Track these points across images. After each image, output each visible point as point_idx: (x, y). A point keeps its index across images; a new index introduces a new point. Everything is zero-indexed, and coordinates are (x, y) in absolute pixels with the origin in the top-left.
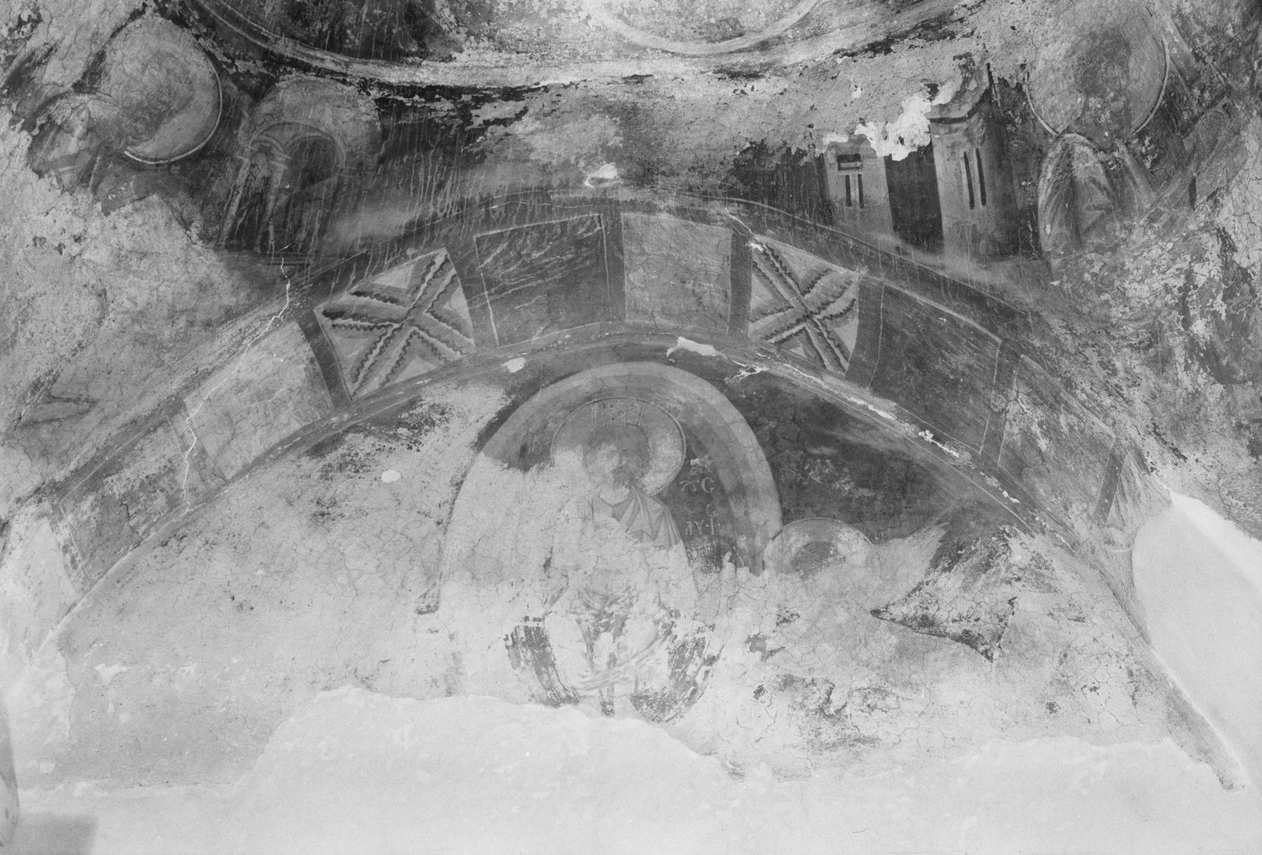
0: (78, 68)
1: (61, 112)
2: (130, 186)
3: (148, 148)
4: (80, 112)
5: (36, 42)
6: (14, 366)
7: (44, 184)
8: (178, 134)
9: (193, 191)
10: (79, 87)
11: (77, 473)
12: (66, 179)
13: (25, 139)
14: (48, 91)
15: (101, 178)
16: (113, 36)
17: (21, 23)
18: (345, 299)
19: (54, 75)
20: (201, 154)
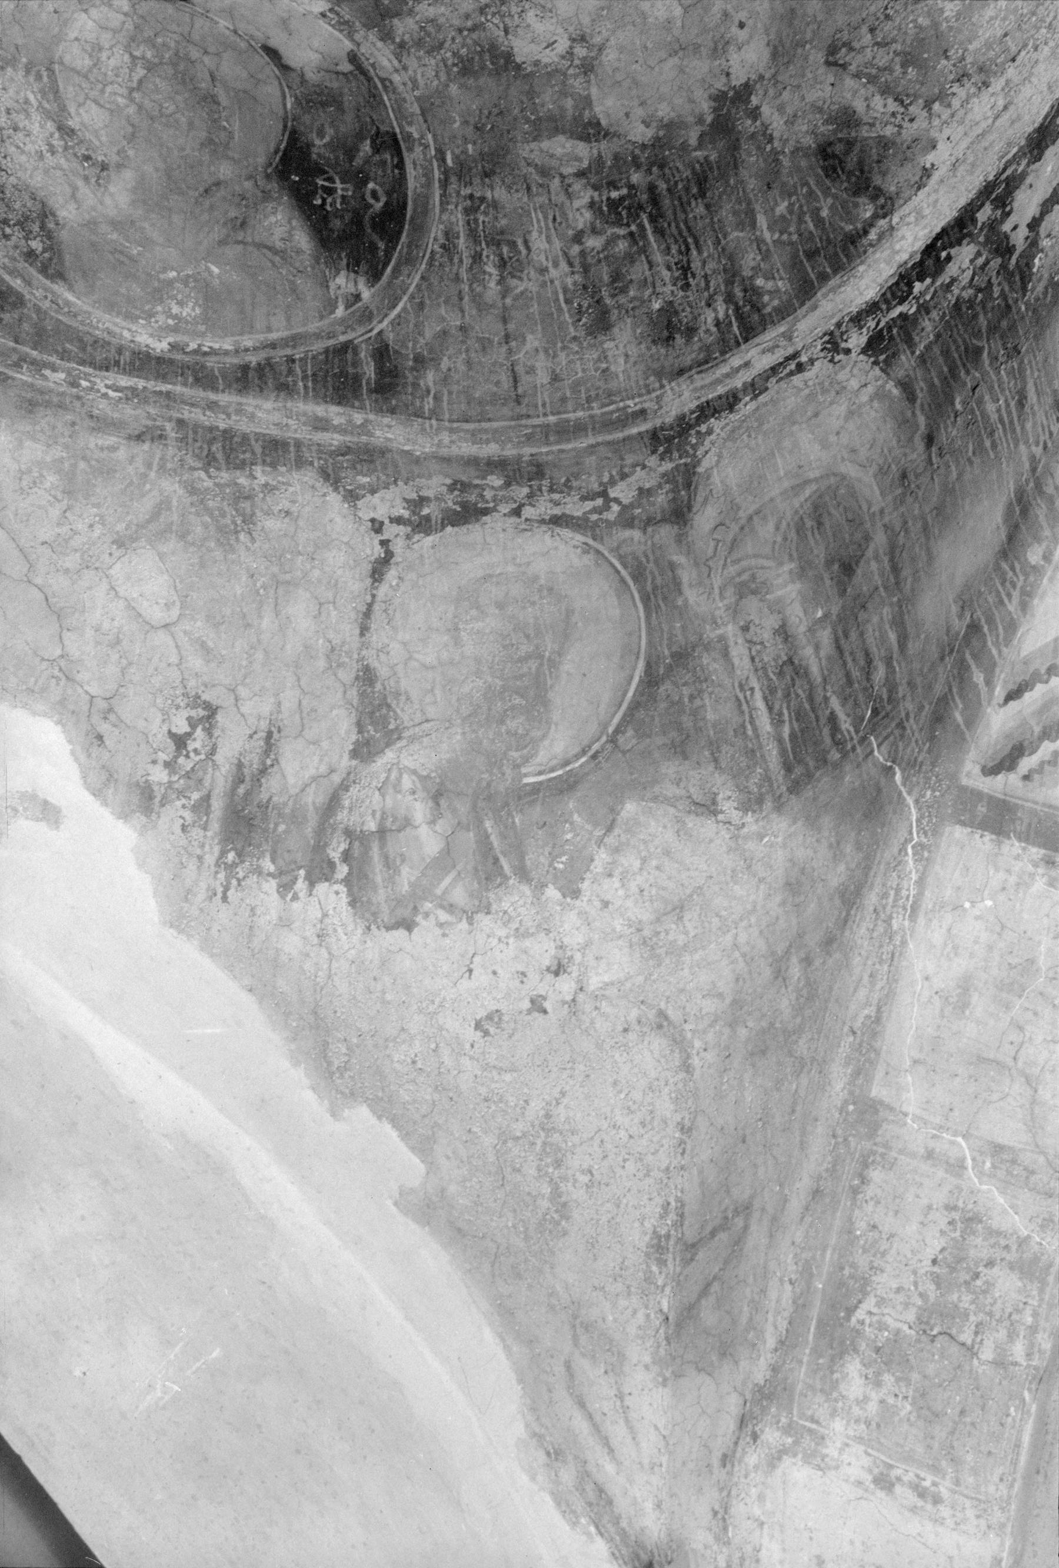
0: (343, 726)
1: (363, 809)
2: (577, 822)
3: (557, 745)
4: (395, 786)
5: (234, 742)
6: (592, 1244)
7: (426, 931)
8: (590, 686)
9: (680, 749)
10: (364, 751)
11: (786, 1345)
12: (459, 896)
13: (332, 897)
14: (315, 798)
15: (518, 850)
16: (364, 630)
17: (180, 742)
18: (998, 722)
19: (300, 771)
20: (651, 681)
